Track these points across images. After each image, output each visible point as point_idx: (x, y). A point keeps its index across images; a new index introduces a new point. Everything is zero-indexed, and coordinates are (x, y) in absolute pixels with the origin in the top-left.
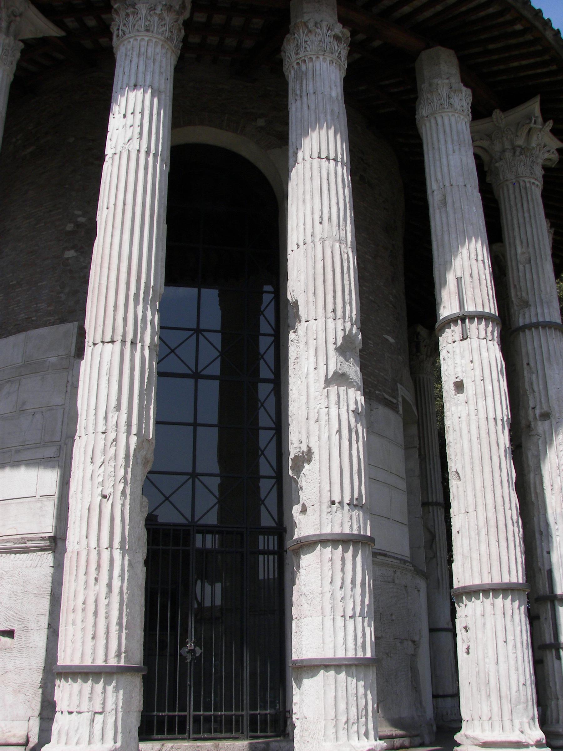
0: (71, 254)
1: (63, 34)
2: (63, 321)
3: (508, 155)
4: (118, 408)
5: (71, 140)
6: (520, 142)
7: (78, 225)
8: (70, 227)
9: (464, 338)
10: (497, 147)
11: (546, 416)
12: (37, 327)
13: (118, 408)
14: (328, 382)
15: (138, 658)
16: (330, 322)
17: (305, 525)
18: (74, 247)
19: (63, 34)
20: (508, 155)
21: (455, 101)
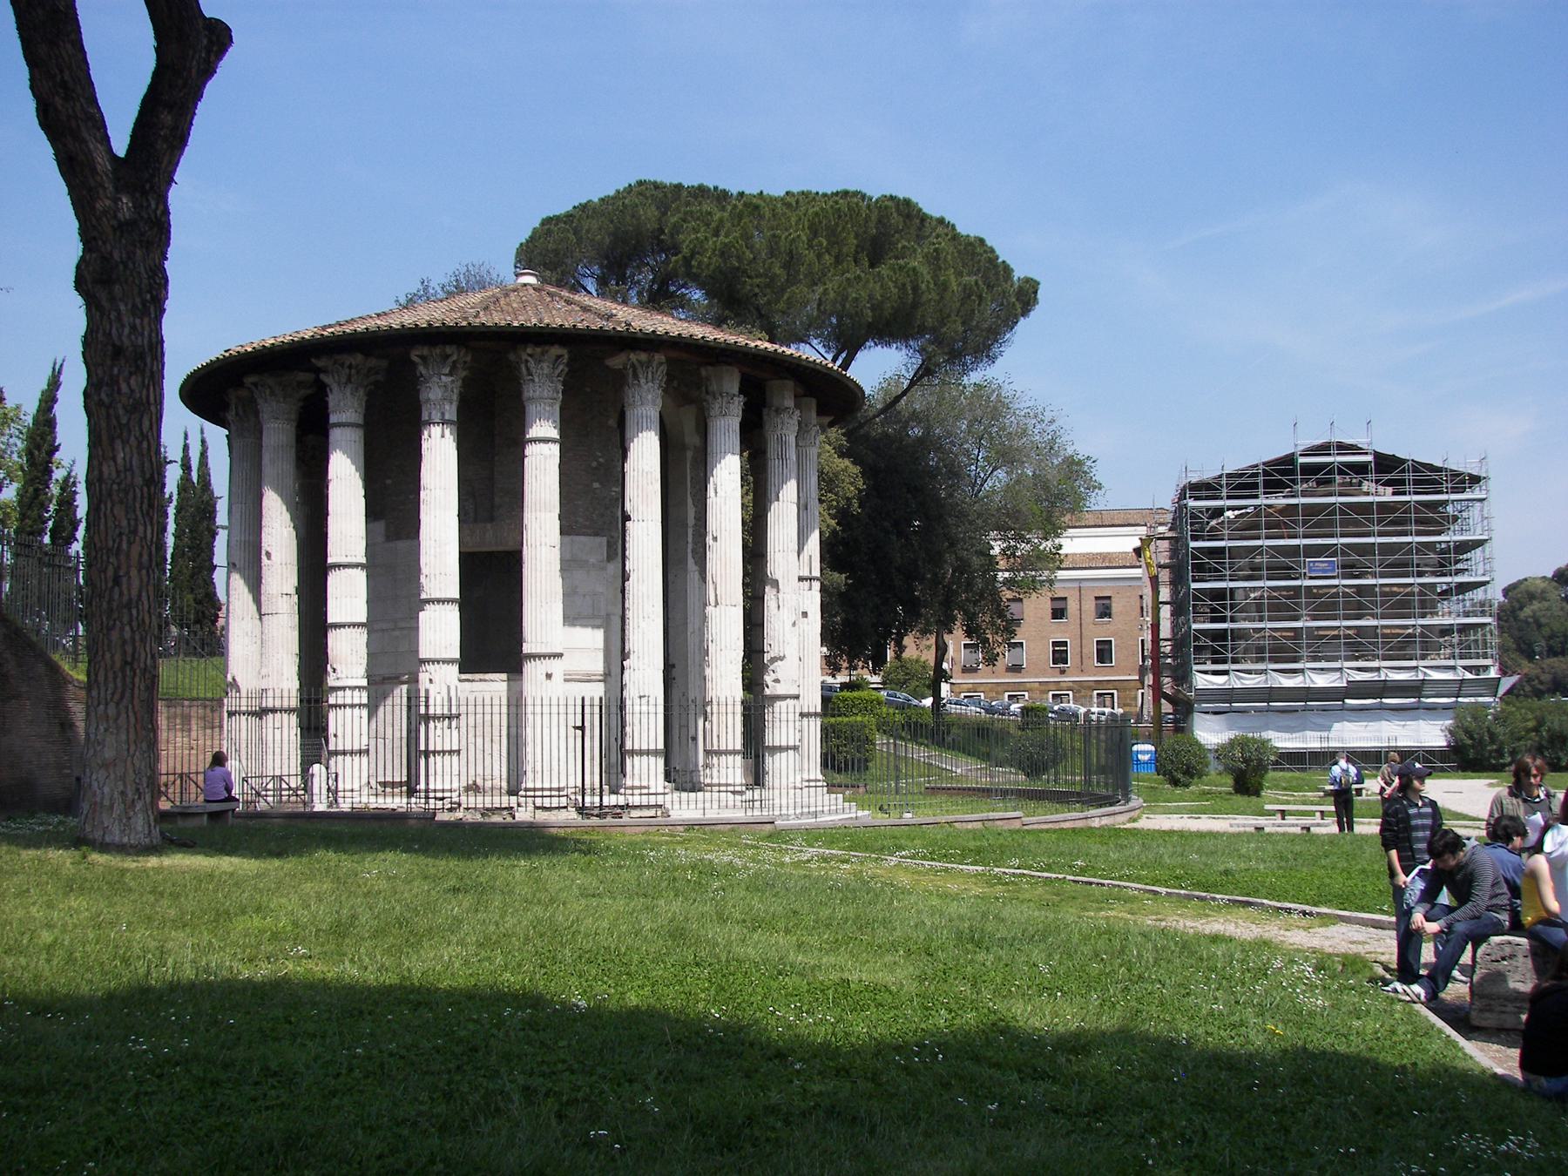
0: (596, 485)
2: (596, 534)
7: (600, 464)
8: (594, 464)
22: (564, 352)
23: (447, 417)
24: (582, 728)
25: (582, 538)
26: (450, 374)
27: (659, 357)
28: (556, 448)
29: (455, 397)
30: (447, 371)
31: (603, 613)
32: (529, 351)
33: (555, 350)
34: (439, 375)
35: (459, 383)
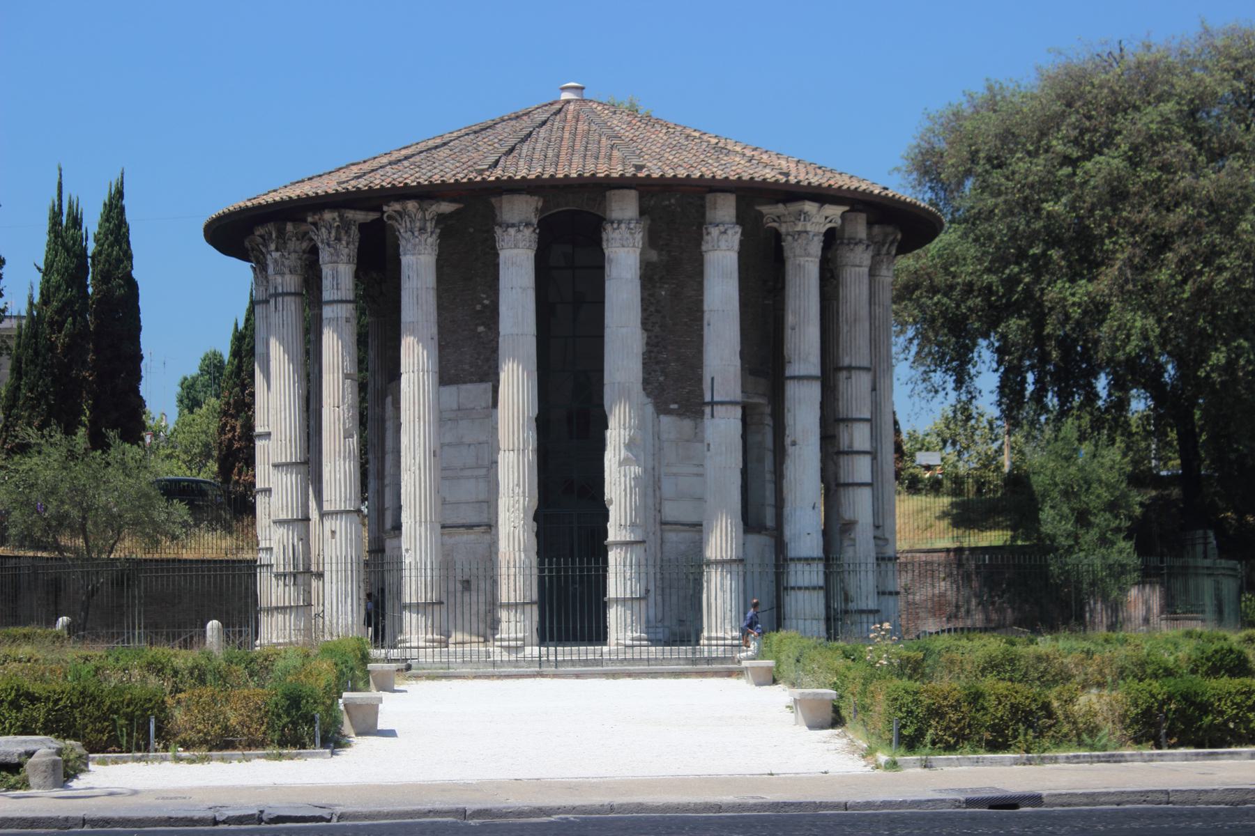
0: (481, 329)
1: (462, 206)
2: (481, 380)
3: (790, 238)
4: (518, 485)
5: (471, 230)
6: (799, 228)
7: (485, 306)
8: (478, 307)
9: (712, 416)
10: (783, 229)
11: (794, 444)
12: (465, 383)
13: (518, 485)
14: (620, 464)
15: (535, 597)
16: (622, 432)
17: (612, 537)
18: (483, 324)
19: (462, 206)
20: (790, 238)
21: (723, 245)
22: (336, 215)
23: (280, 290)
24: (468, 582)
25: (469, 386)
26: (277, 250)
27: (411, 205)
28: (346, 311)
29: (287, 271)
30: (273, 247)
31: (486, 463)
32: (310, 219)
33: (328, 215)
34: (269, 252)
35: (293, 256)
